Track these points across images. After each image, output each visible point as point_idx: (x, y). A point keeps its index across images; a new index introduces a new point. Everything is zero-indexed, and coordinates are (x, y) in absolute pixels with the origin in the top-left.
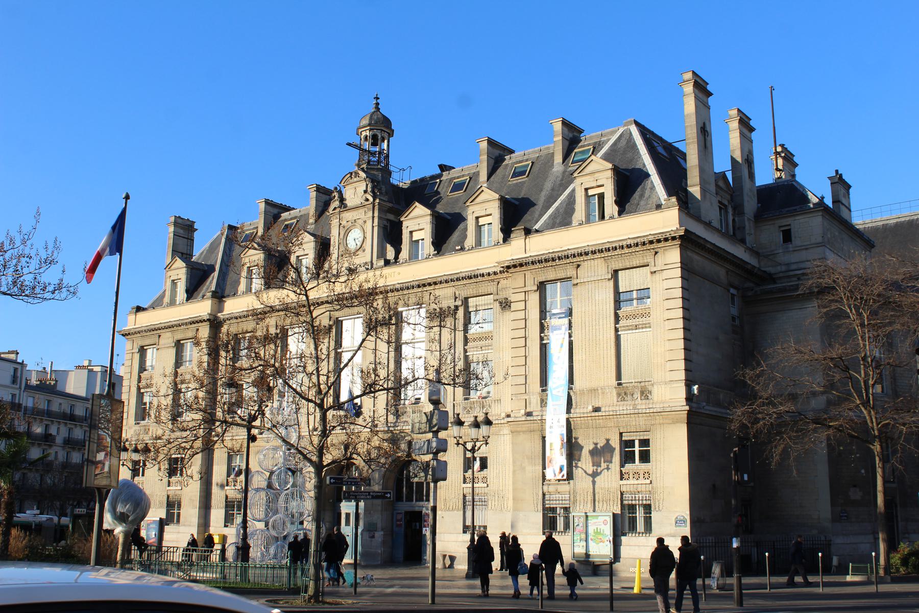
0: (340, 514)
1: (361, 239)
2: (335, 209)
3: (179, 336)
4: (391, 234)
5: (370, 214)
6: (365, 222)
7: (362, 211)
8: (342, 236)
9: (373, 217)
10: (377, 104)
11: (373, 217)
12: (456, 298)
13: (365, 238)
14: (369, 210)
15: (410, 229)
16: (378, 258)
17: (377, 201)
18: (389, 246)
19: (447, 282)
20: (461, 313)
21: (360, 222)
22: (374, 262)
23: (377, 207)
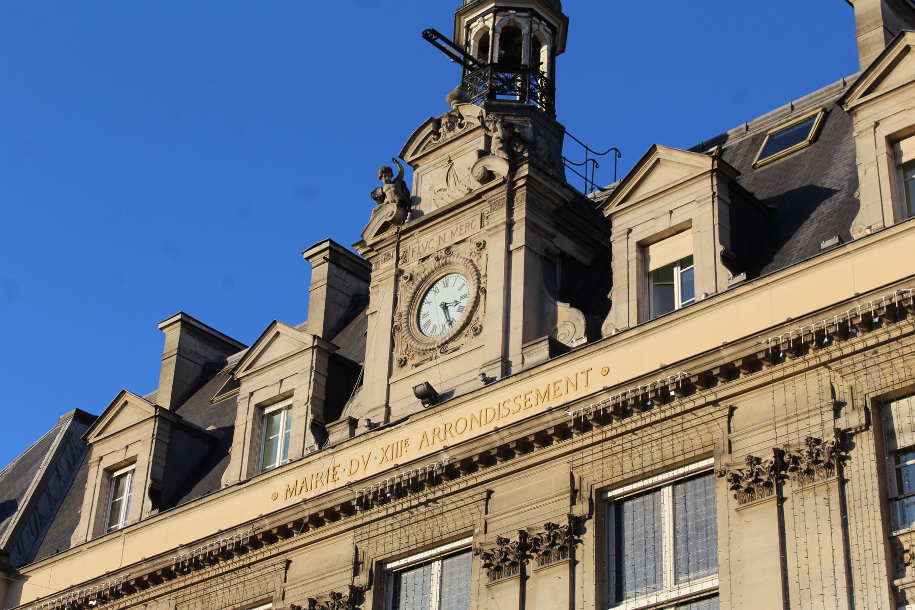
1: (467, 303)
2: (385, 227)
5: (500, 215)
6: (481, 246)
7: (471, 217)
8: (403, 307)
9: (510, 225)
11: (510, 225)
12: (838, 407)
13: (481, 290)
14: (494, 207)
15: (636, 237)
16: (529, 338)
17: (524, 170)
19: (798, 348)
20: (863, 458)
21: (466, 250)
22: (515, 357)
23: (521, 196)
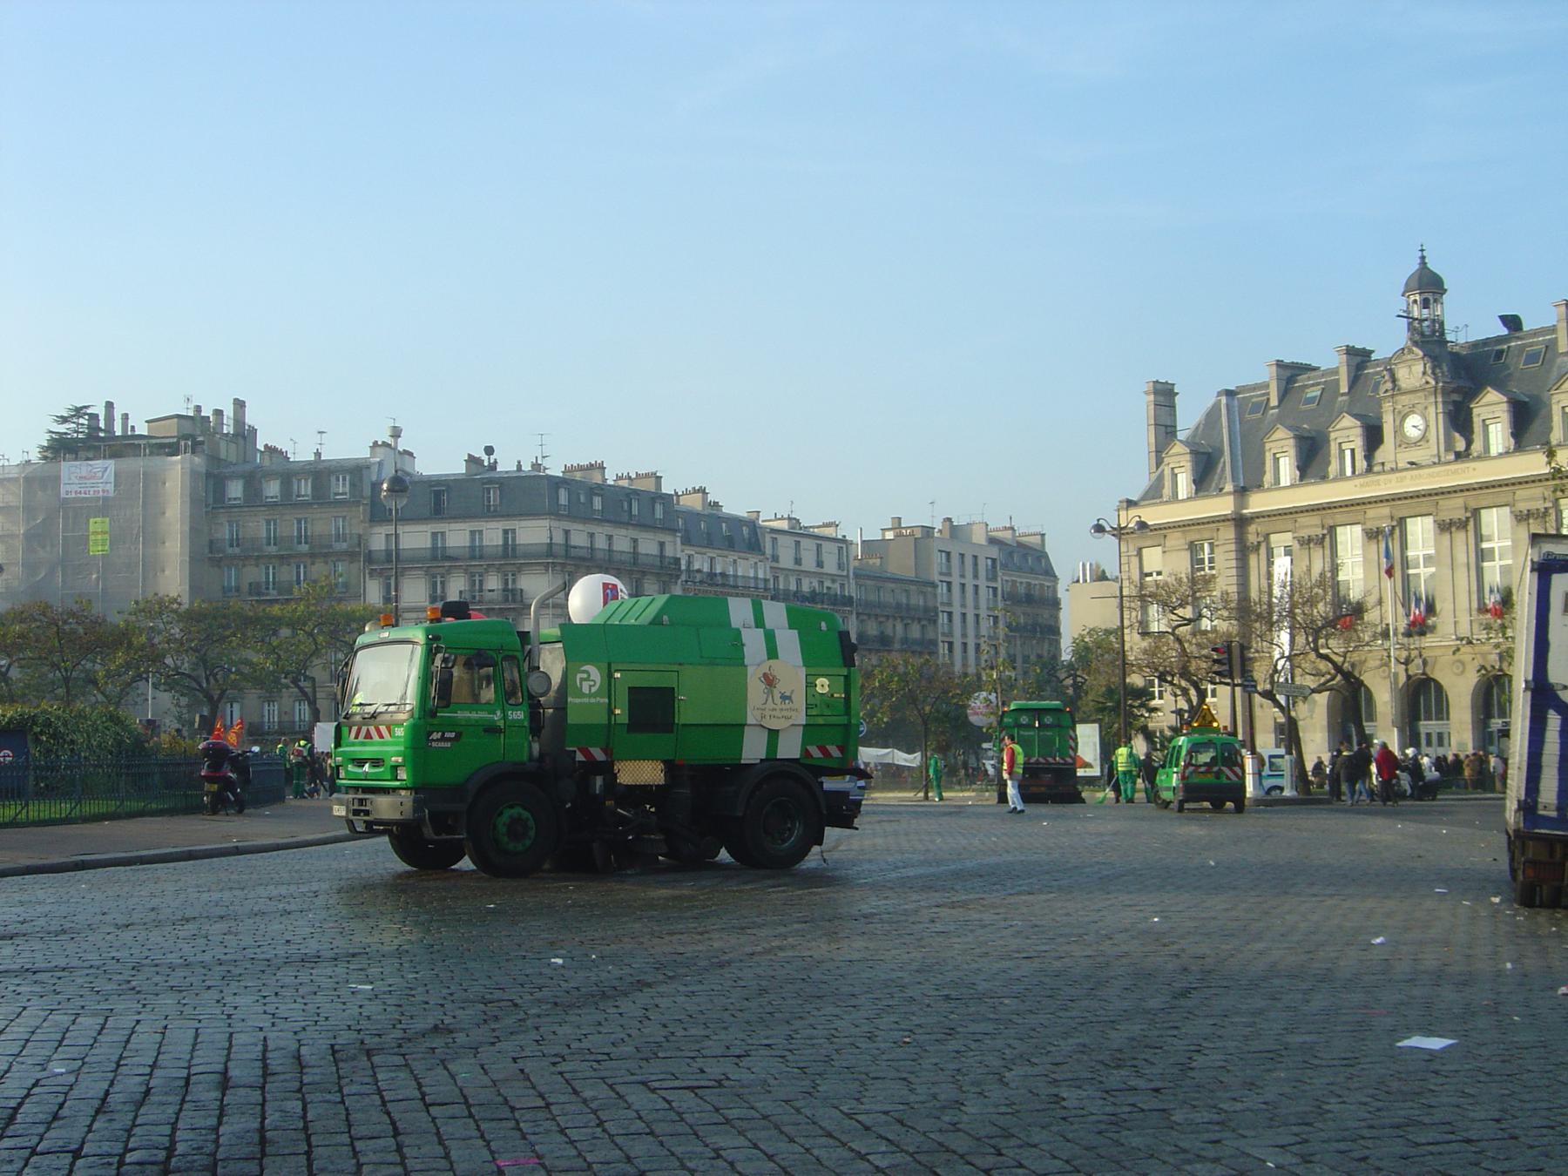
0: (1418, 734)
3: (1192, 536)
4: (1460, 420)
10: (1423, 258)
13: (1427, 426)
16: (1447, 450)
18: (1457, 435)
